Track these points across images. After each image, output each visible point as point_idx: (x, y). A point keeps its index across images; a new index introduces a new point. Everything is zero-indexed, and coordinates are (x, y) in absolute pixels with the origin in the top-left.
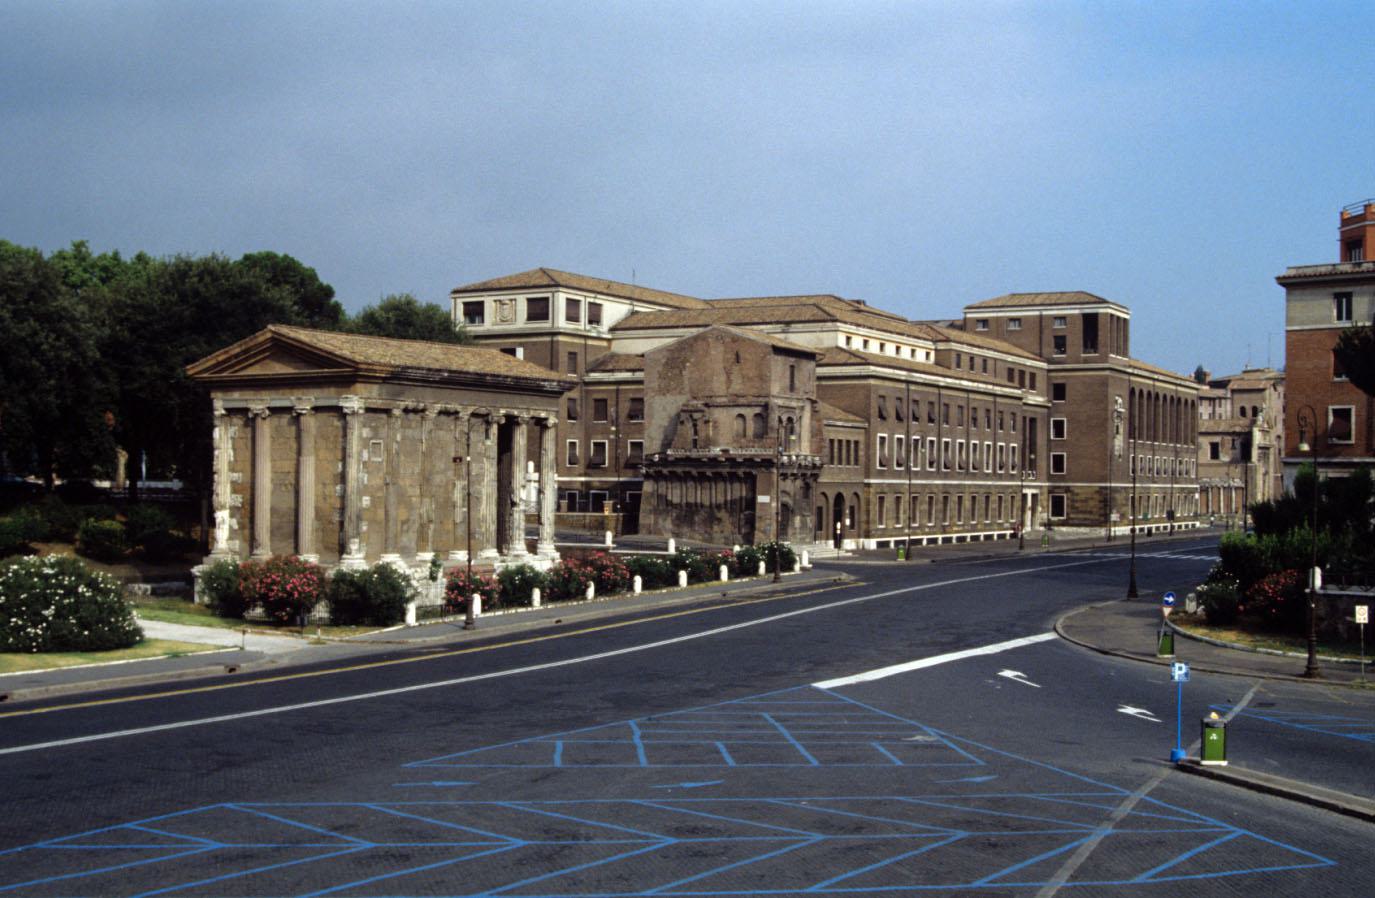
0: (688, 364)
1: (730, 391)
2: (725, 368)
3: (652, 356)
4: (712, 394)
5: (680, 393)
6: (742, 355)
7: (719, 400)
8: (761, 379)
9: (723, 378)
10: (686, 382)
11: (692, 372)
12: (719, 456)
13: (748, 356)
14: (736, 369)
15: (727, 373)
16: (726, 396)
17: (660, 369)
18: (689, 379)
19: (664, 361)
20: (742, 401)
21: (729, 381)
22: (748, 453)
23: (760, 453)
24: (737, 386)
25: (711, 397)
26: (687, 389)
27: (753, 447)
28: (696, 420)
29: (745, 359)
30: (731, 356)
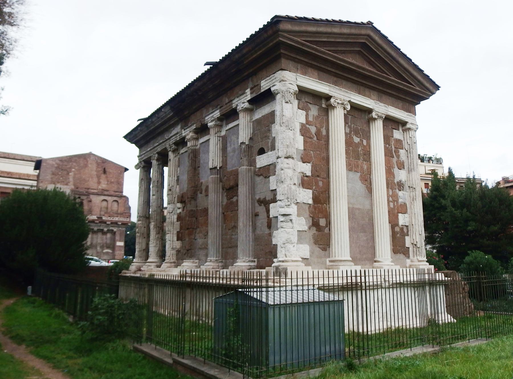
0: (73, 170)
1: (100, 187)
2: (97, 175)
3: (51, 162)
4: (88, 187)
5: (67, 184)
6: (107, 170)
7: (93, 191)
8: (118, 183)
9: (95, 180)
10: (71, 179)
11: (75, 174)
12: (96, 220)
13: (111, 171)
14: (103, 176)
15: (97, 177)
16: (98, 189)
17: (54, 169)
18: (74, 178)
19: (56, 165)
20: (106, 193)
21: (99, 183)
22: (114, 219)
23: (121, 220)
24: (103, 185)
25: (88, 189)
26: (72, 183)
27: (117, 217)
28: (83, 200)
29: (110, 173)
30: (101, 169)
